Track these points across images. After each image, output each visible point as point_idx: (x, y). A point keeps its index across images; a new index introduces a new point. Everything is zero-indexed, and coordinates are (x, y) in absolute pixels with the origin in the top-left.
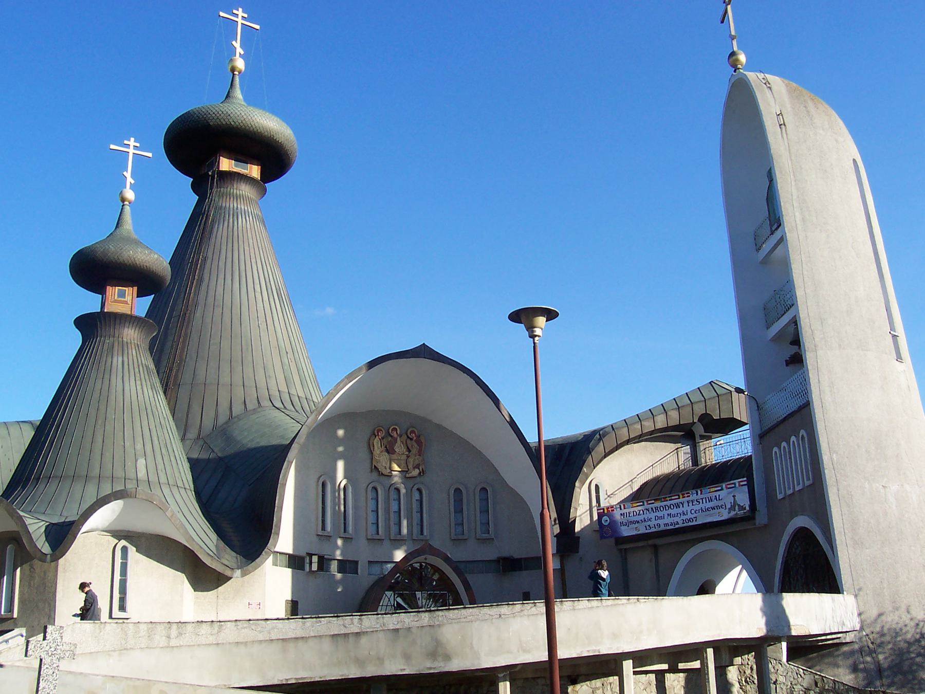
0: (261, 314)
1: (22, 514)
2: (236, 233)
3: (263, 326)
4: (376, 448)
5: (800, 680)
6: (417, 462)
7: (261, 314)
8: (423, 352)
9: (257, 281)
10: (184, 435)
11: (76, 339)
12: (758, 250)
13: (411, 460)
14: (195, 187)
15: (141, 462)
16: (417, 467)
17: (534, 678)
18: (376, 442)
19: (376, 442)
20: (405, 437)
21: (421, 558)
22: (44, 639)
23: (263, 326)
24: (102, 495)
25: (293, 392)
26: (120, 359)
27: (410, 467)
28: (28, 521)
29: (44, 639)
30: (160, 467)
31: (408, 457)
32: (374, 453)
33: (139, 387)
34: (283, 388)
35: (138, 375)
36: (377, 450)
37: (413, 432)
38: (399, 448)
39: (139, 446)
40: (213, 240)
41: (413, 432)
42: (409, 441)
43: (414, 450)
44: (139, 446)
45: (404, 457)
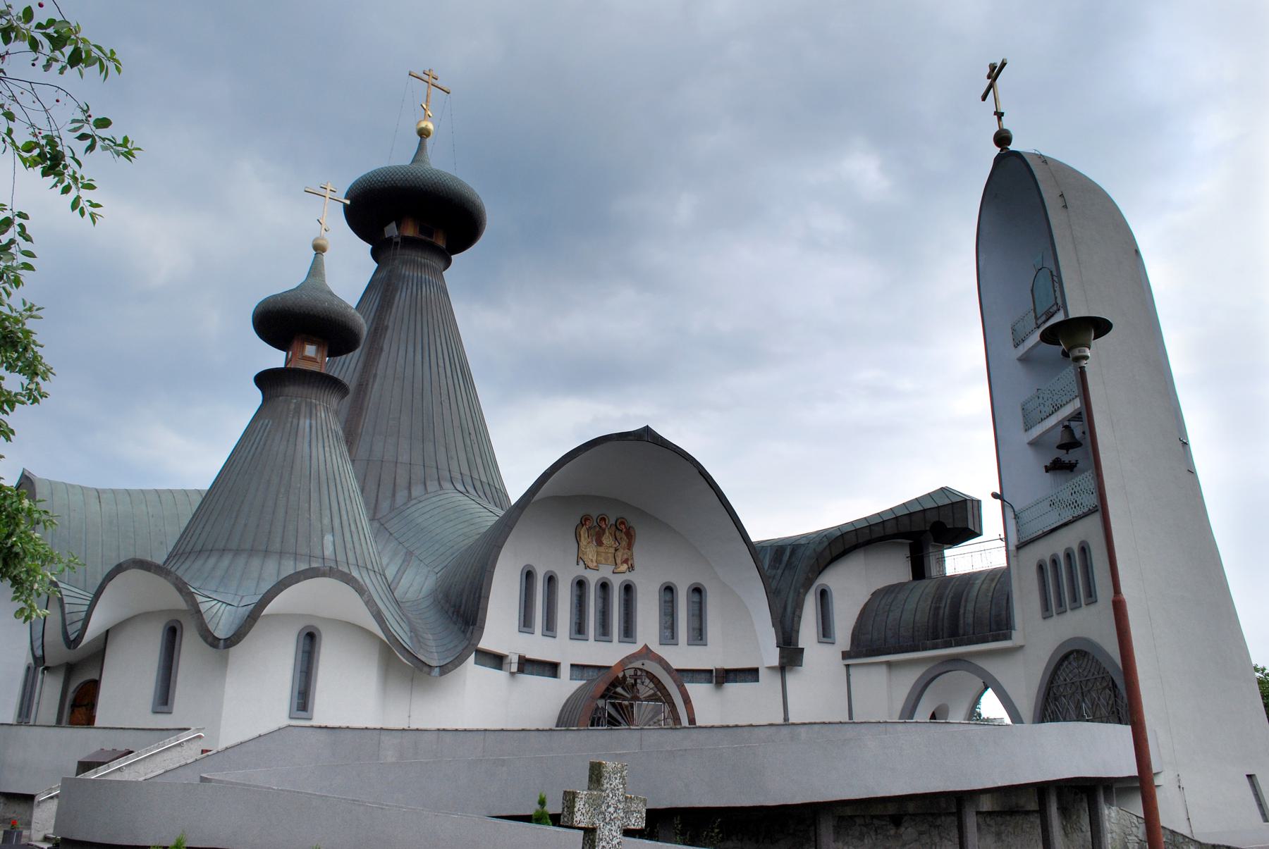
0: (444, 392)
3: (446, 404)
5: (1134, 830)
7: (444, 392)
8: (646, 435)
9: (440, 355)
10: (375, 513)
11: (257, 396)
12: (1016, 346)
13: (619, 554)
14: (375, 255)
15: (328, 538)
16: (626, 561)
17: (851, 817)
18: (583, 532)
19: (583, 532)
22: (628, 833)
23: (446, 404)
24: (284, 574)
25: (475, 476)
26: (308, 422)
27: (619, 561)
28: (199, 599)
29: (628, 833)
30: (349, 546)
33: (327, 455)
34: (465, 470)
36: (583, 542)
37: (623, 523)
38: (607, 540)
39: (326, 521)
40: (394, 310)
42: (618, 533)
43: (624, 543)
44: (326, 521)
45: (612, 550)
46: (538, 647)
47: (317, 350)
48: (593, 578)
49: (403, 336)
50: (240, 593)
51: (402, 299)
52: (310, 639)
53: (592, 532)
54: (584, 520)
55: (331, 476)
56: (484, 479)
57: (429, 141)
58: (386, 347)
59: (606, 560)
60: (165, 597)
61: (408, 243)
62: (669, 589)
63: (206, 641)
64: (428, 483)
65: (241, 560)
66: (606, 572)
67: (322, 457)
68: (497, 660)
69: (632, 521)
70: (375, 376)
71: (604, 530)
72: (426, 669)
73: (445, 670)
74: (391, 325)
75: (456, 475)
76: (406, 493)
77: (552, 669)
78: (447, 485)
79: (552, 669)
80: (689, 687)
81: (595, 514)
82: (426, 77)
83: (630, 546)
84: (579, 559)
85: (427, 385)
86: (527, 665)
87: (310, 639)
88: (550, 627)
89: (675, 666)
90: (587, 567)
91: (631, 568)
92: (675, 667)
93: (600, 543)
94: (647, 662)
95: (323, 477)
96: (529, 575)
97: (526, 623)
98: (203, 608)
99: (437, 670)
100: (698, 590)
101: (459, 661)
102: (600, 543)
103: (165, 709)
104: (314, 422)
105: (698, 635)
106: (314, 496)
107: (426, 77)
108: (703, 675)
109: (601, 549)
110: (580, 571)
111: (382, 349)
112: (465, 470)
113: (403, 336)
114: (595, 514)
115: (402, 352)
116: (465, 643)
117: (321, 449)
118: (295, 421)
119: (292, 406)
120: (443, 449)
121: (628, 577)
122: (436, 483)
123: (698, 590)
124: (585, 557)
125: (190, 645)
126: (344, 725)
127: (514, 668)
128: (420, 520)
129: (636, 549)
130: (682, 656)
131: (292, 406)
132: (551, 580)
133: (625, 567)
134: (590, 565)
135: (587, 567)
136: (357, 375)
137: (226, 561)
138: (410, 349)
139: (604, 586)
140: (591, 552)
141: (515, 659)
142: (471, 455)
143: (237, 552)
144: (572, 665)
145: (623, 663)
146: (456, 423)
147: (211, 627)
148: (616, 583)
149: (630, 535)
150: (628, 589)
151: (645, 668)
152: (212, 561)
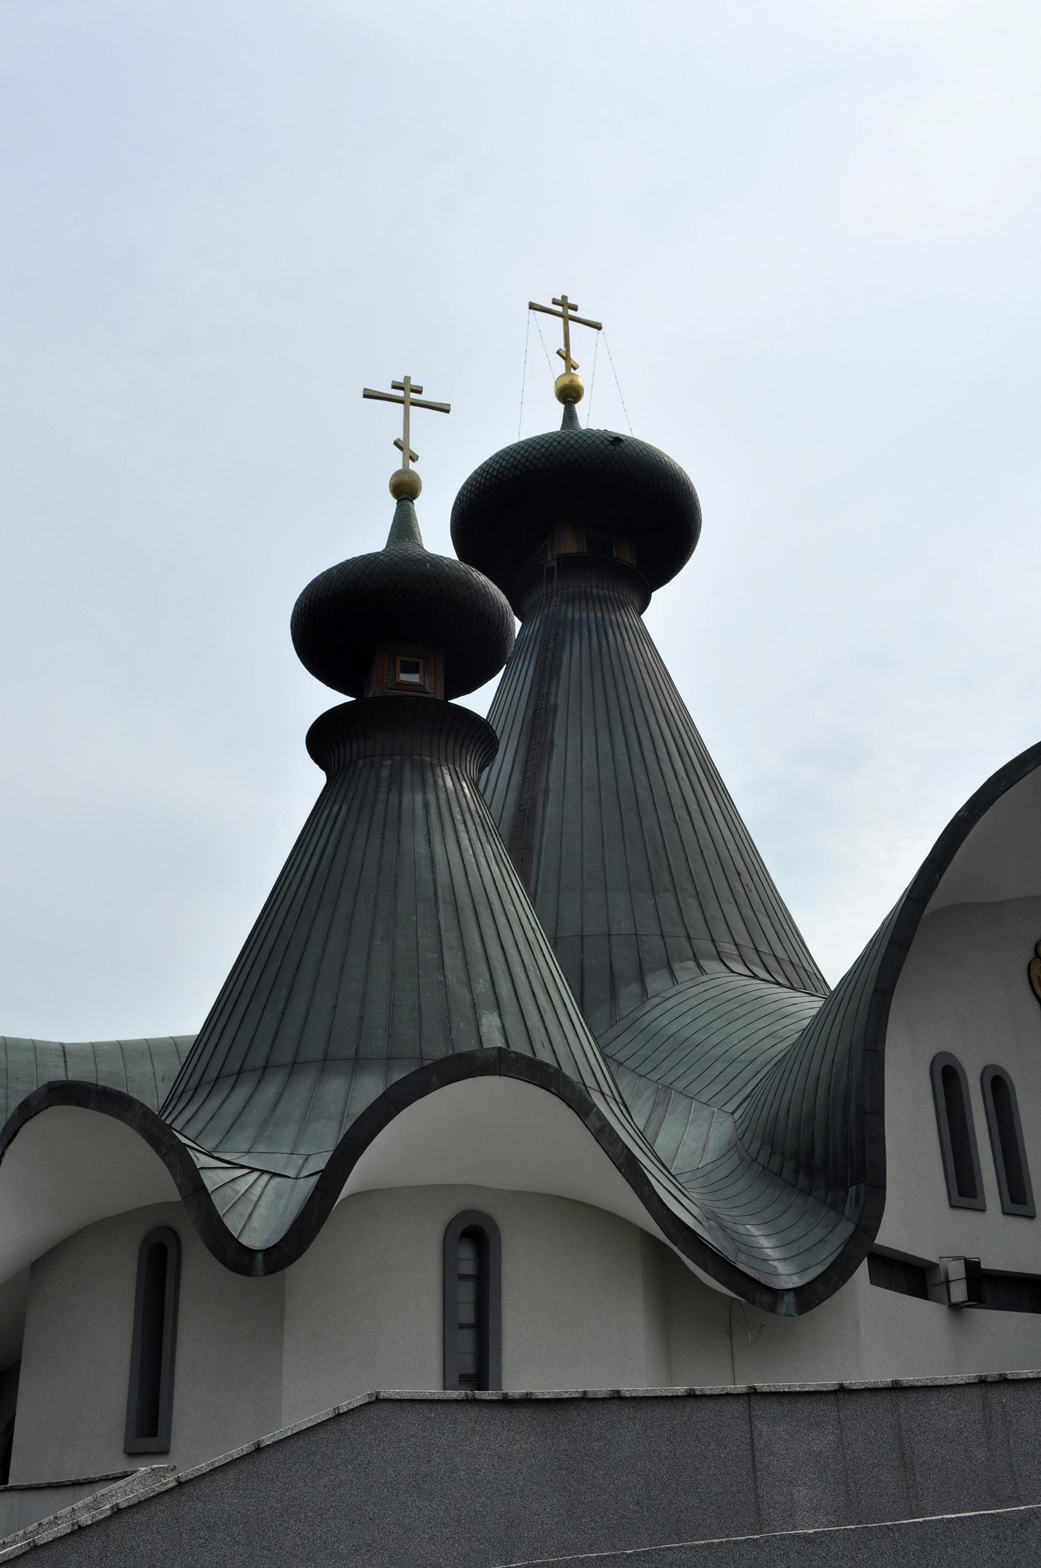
0: (677, 801)
1: (184, 1140)
2: (606, 661)
11: (315, 779)
15: (490, 1022)
25: (764, 948)
26: (419, 798)
28: (202, 1160)
35: (464, 836)
39: (482, 986)
44: (482, 986)
47: (423, 678)
50: (303, 1150)
51: (573, 656)
52: (474, 1242)
55: (480, 898)
56: (781, 954)
57: (578, 407)
58: (558, 740)
60: (139, 1179)
61: (570, 565)
63: (223, 1260)
64: (676, 966)
65: (303, 1085)
67: (455, 860)
68: (910, 1276)
70: (546, 791)
72: (766, 1299)
73: (810, 1297)
74: (561, 703)
75: (728, 947)
76: (635, 988)
78: (713, 966)
82: (559, 309)
85: (644, 794)
87: (474, 1242)
95: (464, 900)
96: (947, 1078)
98: (211, 1180)
99: (790, 1299)
101: (836, 1276)
103: (151, 1443)
104: (431, 797)
106: (450, 937)
107: (559, 309)
111: (552, 744)
112: (743, 939)
115: (588, 743)
116: (847, 1229)
117: (452, 847)
118: (394, 798)
119: (385, 773)
120: (693, 902)
122: (691, 964)
125: (199, 1276)
126: (599, 1388)
127: (959, 1293)
128: (673, 1028)
131: (385, 773)
136: (512, 796)
137: (270, 1090)
141: (957, 1271)
142: (748, 912)
143: (294, 1068)
146: (711, 856)
147: (233, 1224)
152: (241, 1094)
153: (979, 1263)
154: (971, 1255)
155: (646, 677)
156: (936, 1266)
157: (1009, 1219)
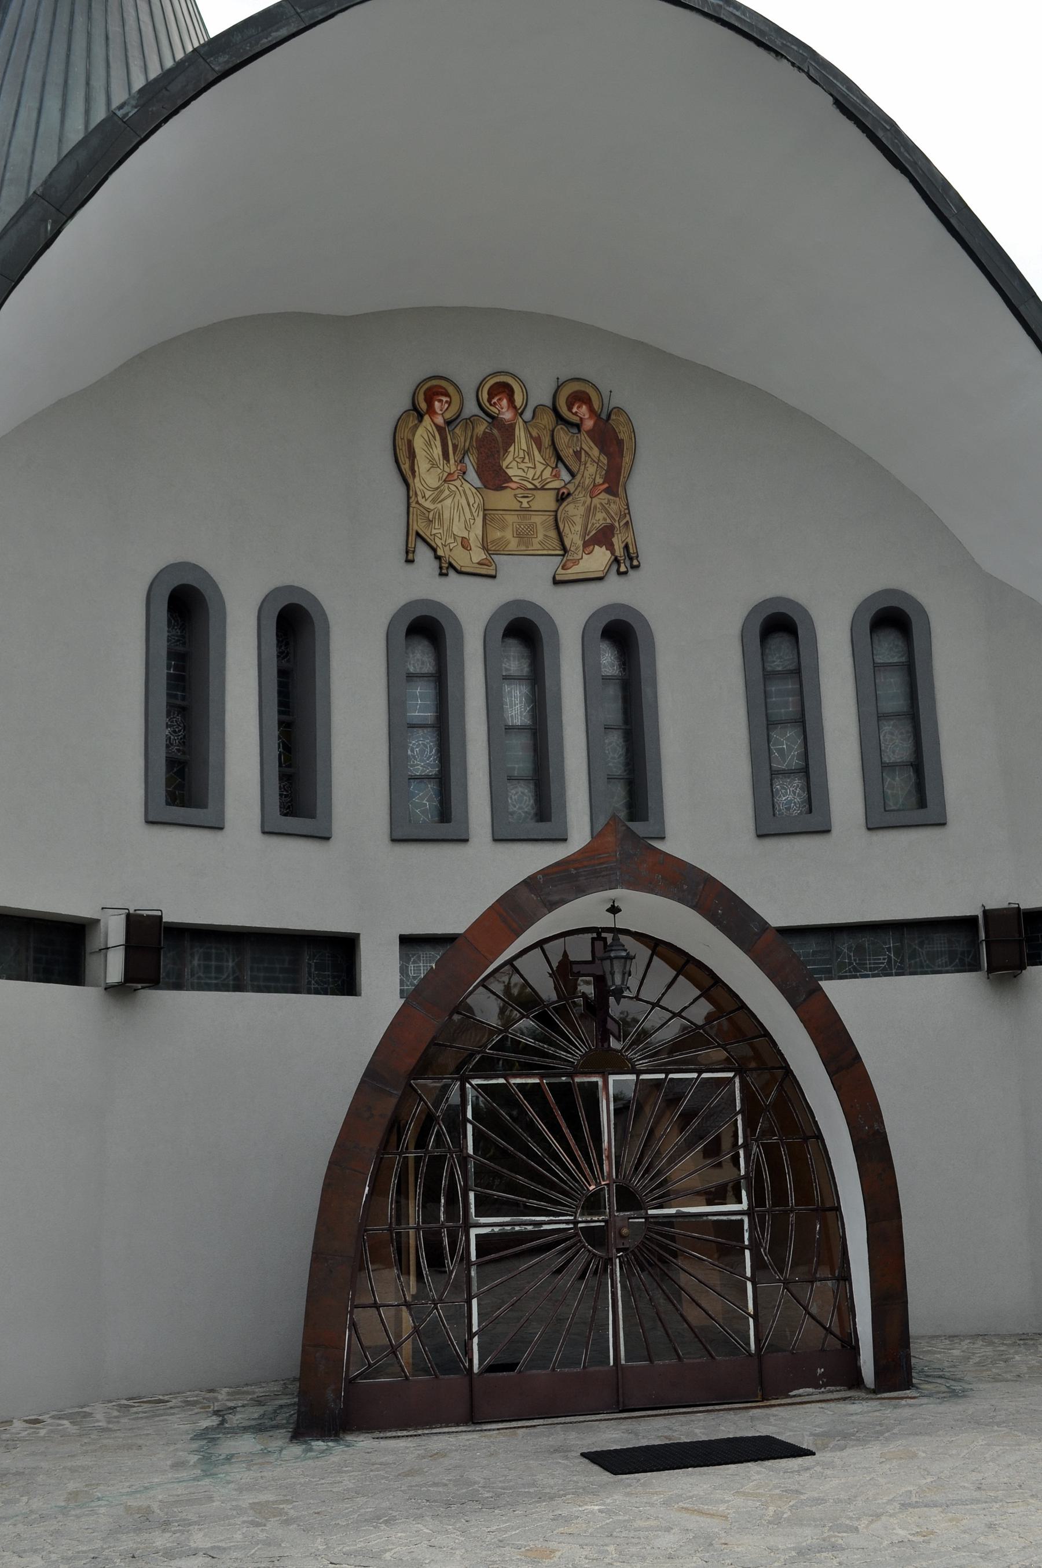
4: (422, 464)
6: (600, 519)
13: (574, 510)
16: (603, 537)
18: (424, 439)
19: (424, 439)
20: (547, 420)
21: (586, 910)
27: (574, 538)
31: (562, 498)
32: (417, 484)
37: (580, 398)
38: (523, 463)
41: (580, 398)
42: (563, 437)
43: (591, 472)
45: (545, 501)
46: (235, 873)
48: (473, 608)
49: (33, 75)
53: (460, 436)
54: (431, 392)
59: (524, 536)
62: (778, 627)
66: (525, 580)
69: (621, 389)
71: (509, 436)
77: (326, 961)
79: (326, 961)
80: (840, 993)
81: (468, 373)
83: (614, 481)
84: (415, 541)
86: (164, 953)
88: (297, 795)
89: (777, 912)
90: (446, 568)
91: (627, 561)
92: (776, 918)
93: (494, 477)
94: (621, 894)
96: (185, 609)
97: (183, 784)
100: (892, 621)
102: (494, 477)
105: (910, 791)
108: (940, 942)
109: (503, 499)
110: (422, 584)
113: (33, 75)
114: (468, 373)
121: (616, 592)
123: (892, 621)
124: (436, 533)
127: (115, 969)
129: (644, 487)
130: (849, 874)
132: (293, 629)
133: (599, 559)
134: (461, 558)
135: (446, 568)
138: (52, 105)
139: (523, 631)
140: (459, 512)
141: (115, 931)
144: (406, 941)
145: (512, 911)
148: (570, 616)
149: (612, 439)
150: (621, 634)
151: (622, 921)
153: (161, 917)
154: (145, 904)
155: (145, 17)
156: (98, 921)
157: (275, 841)
